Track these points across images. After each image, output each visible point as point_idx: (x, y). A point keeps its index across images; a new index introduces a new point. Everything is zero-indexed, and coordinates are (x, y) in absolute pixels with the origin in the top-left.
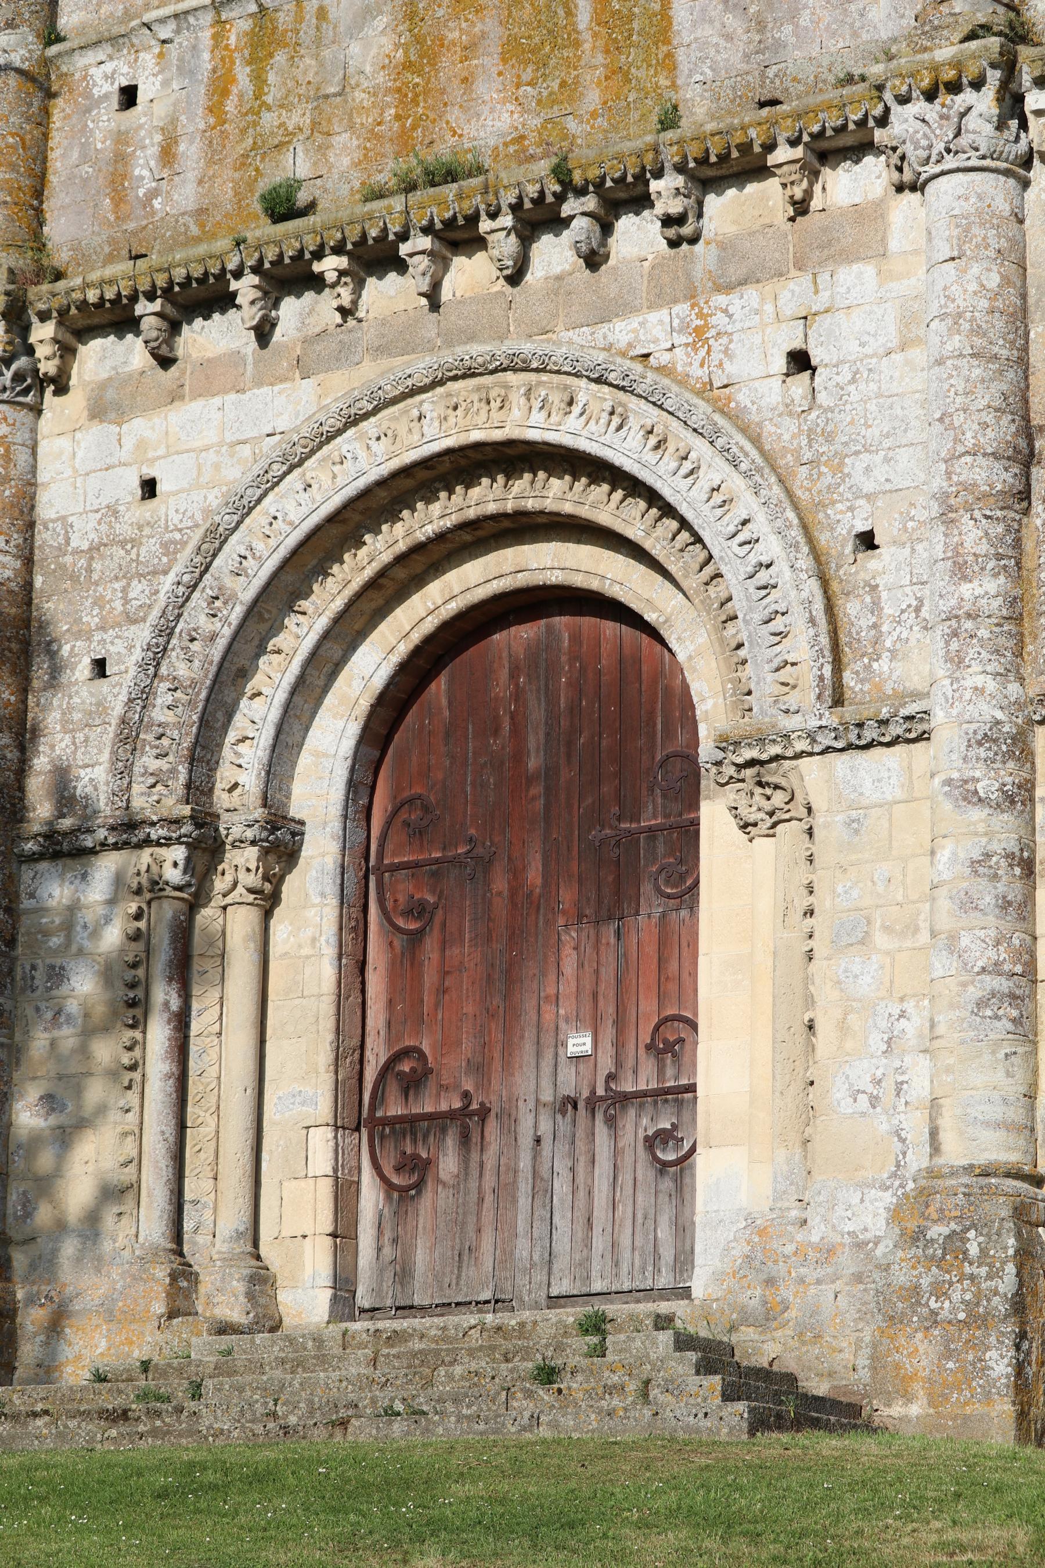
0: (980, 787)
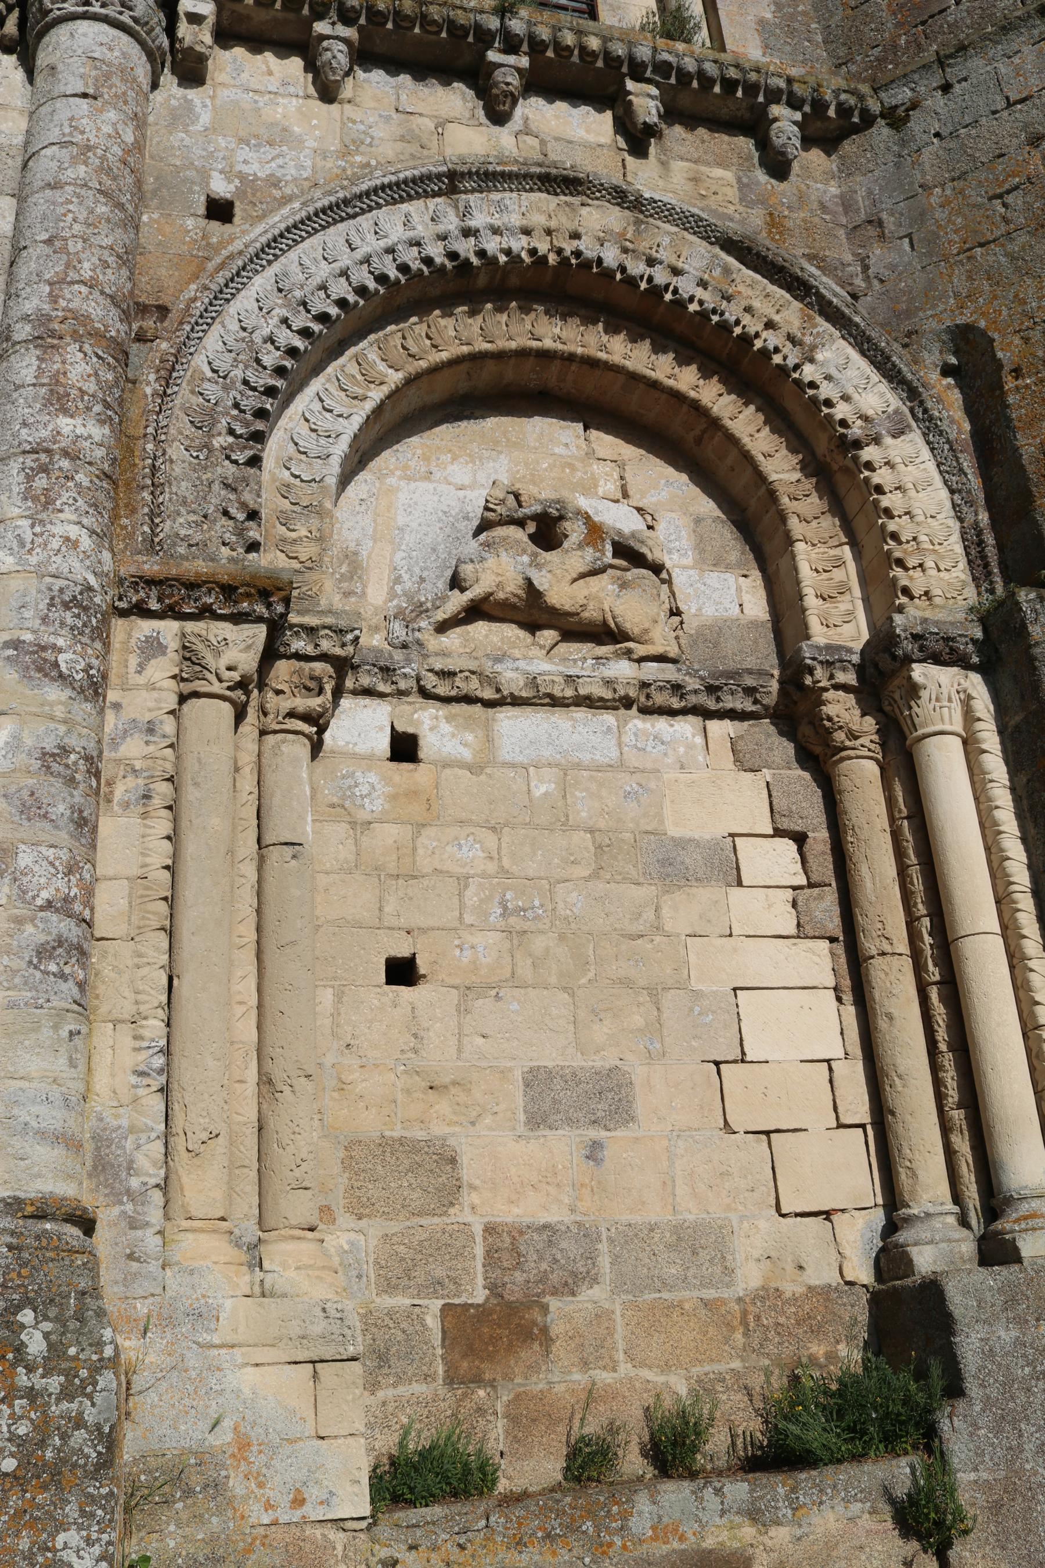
0: (62, 658)
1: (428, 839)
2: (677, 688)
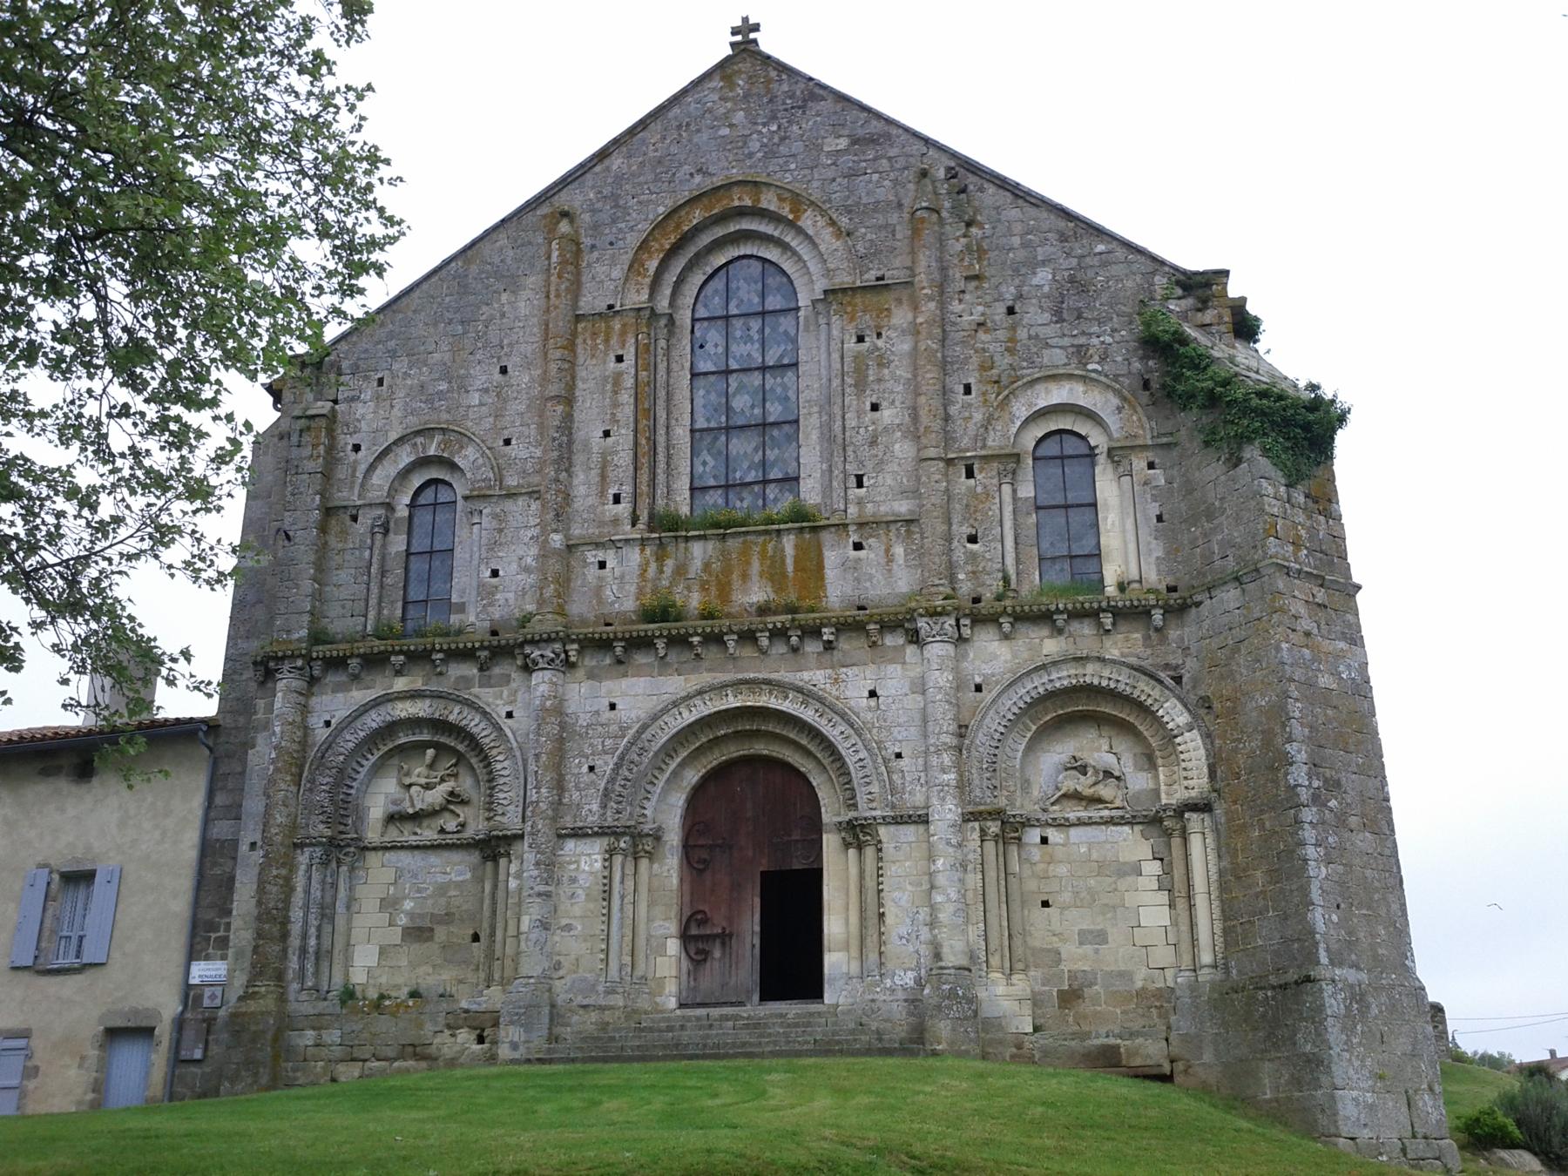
1: (1051, 867)
2: (1122, 817)
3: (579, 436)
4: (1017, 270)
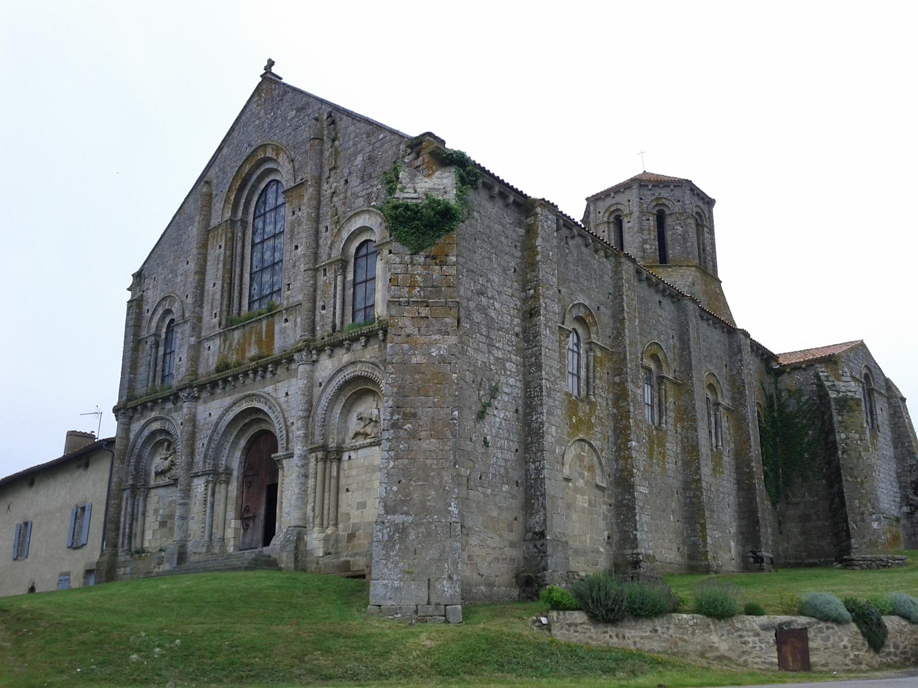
3: (206, 288)
4: (349, 159)
